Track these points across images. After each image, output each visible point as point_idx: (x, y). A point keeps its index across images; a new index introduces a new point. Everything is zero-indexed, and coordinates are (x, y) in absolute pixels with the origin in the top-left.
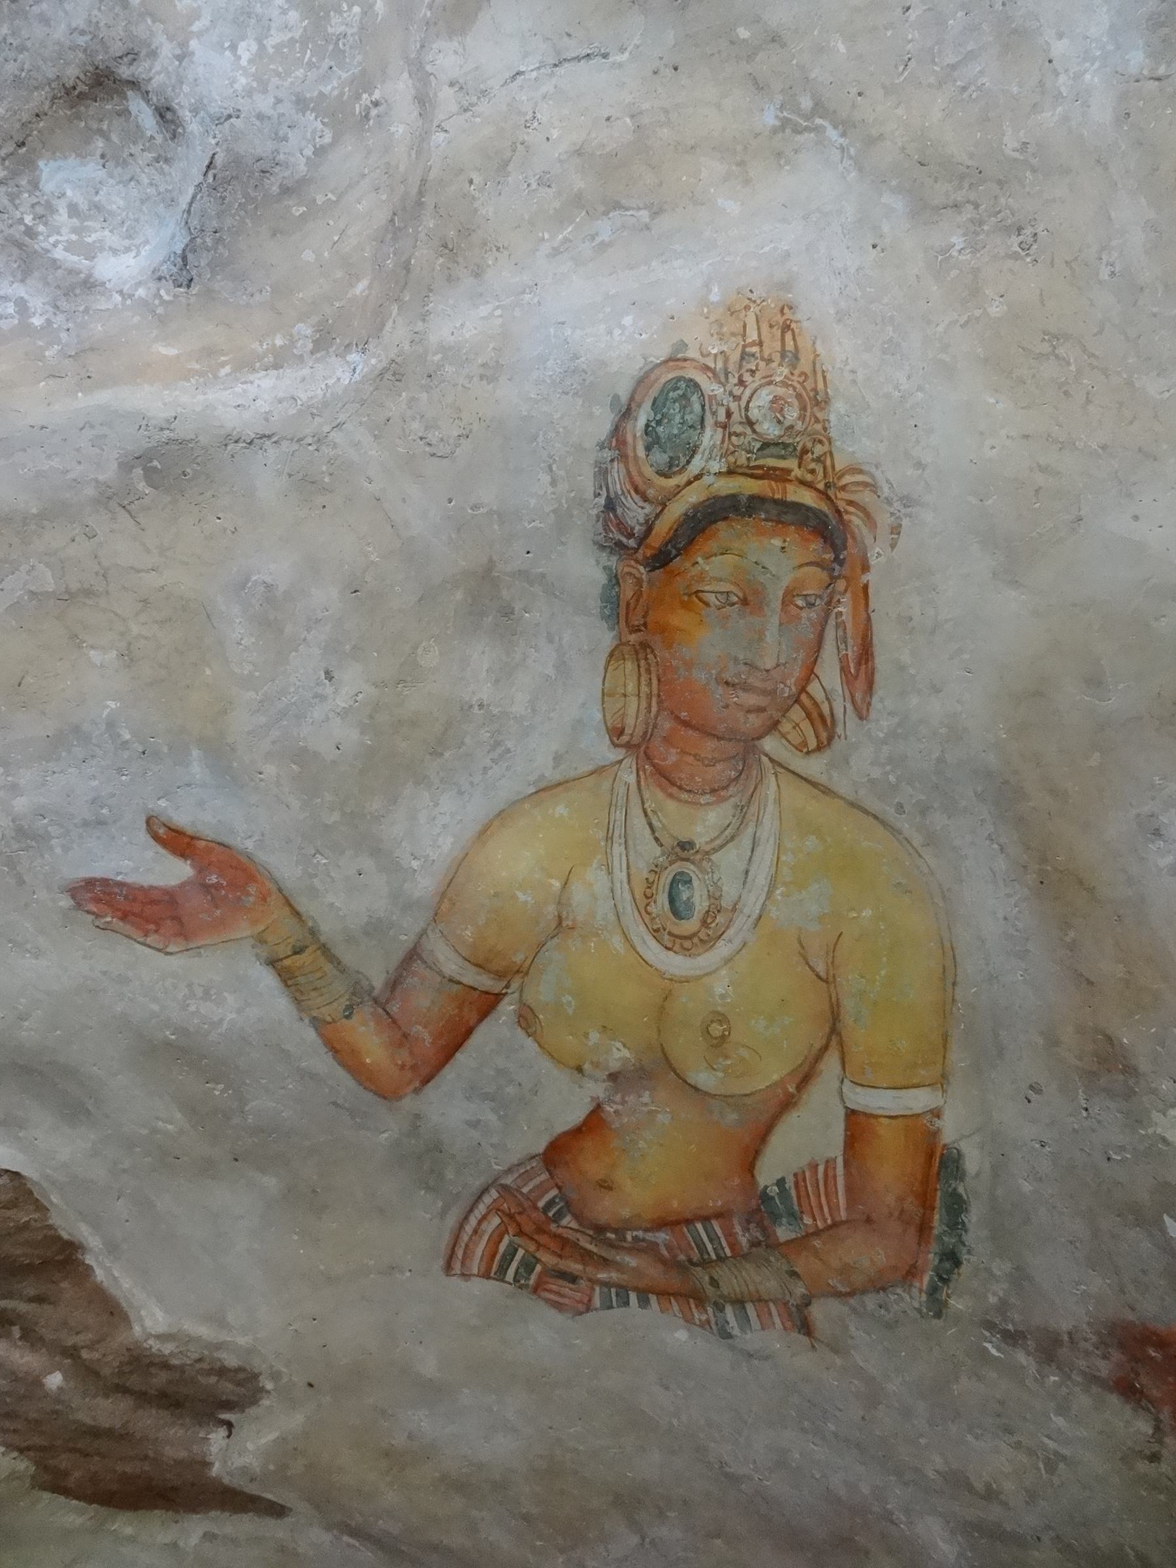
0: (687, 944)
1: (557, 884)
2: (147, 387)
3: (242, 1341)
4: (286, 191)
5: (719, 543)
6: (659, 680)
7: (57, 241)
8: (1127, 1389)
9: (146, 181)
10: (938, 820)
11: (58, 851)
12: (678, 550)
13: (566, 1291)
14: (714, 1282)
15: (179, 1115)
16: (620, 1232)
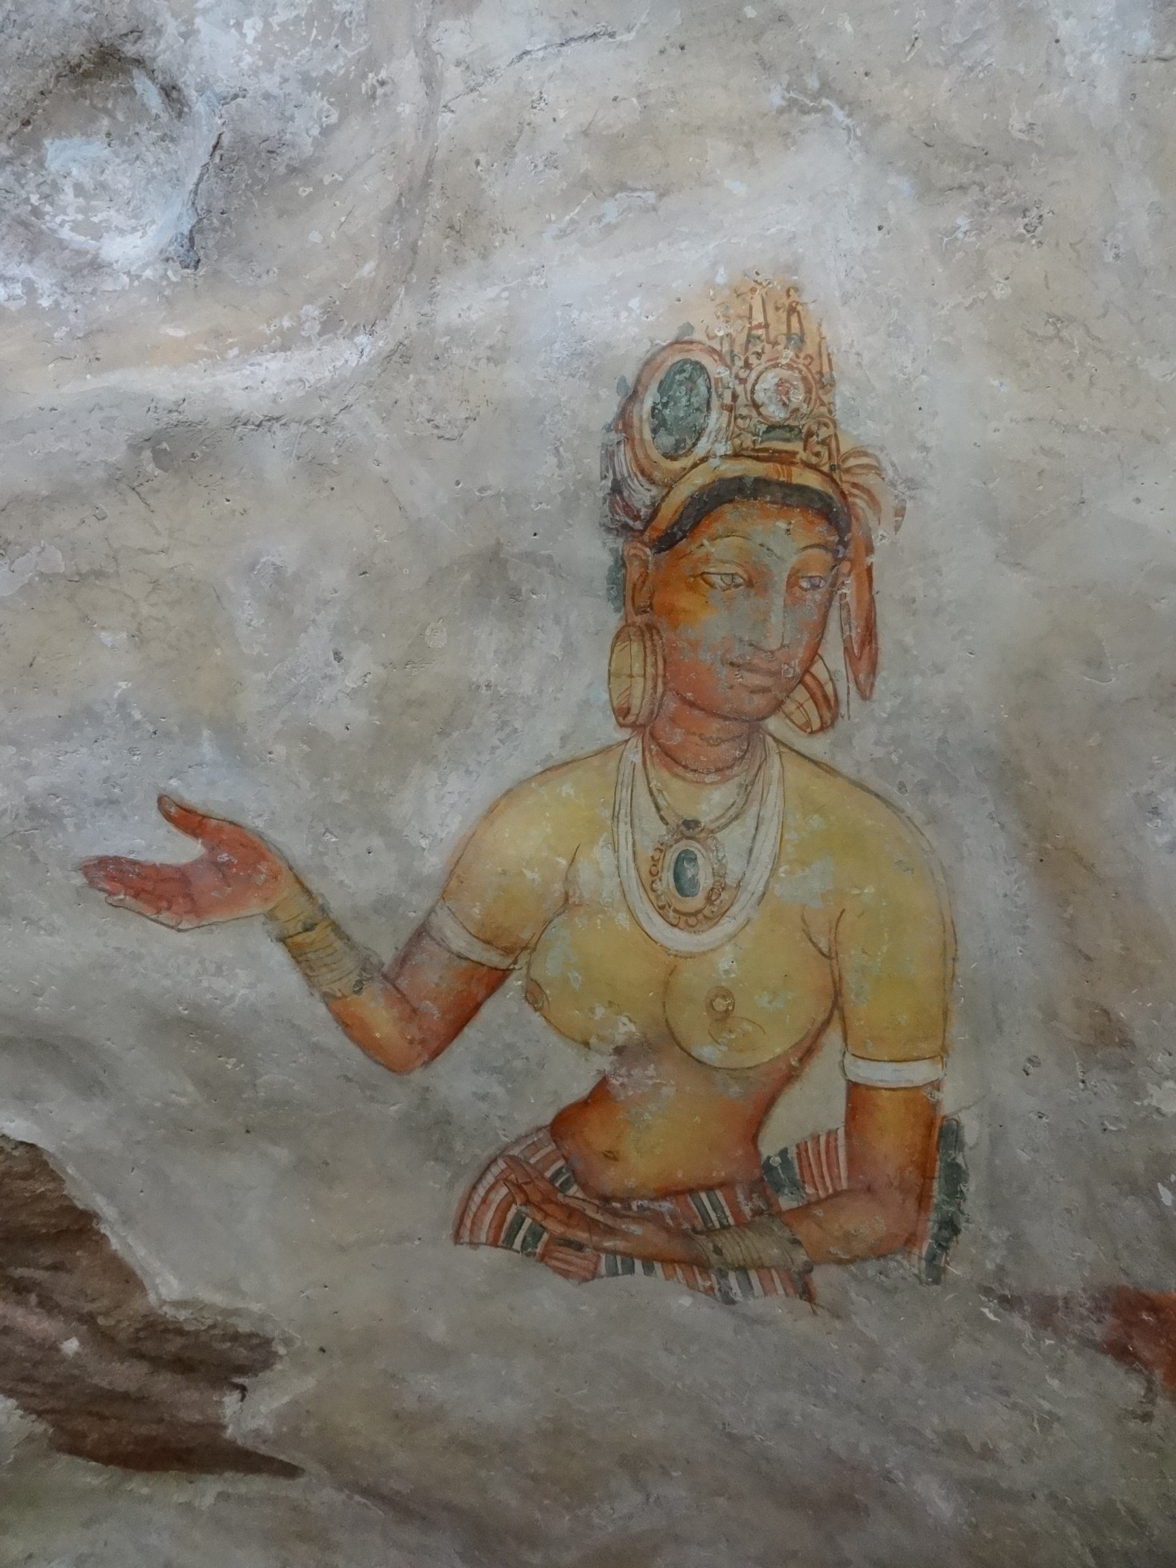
0: (692, 921)
1: (563, 862)
2: (156, 369)
3: (256, 1307)
4: (292, 170)
5: (724, 525)
6: (665, 661)
7: (63, 221)
8: (1121, 1352)
9: (151, 160)
11: (71, 829)
12: (684, 532)
13: (575, 1260)
14: (718, 1251)
15: (191, 1088)
16: (626, 1201)
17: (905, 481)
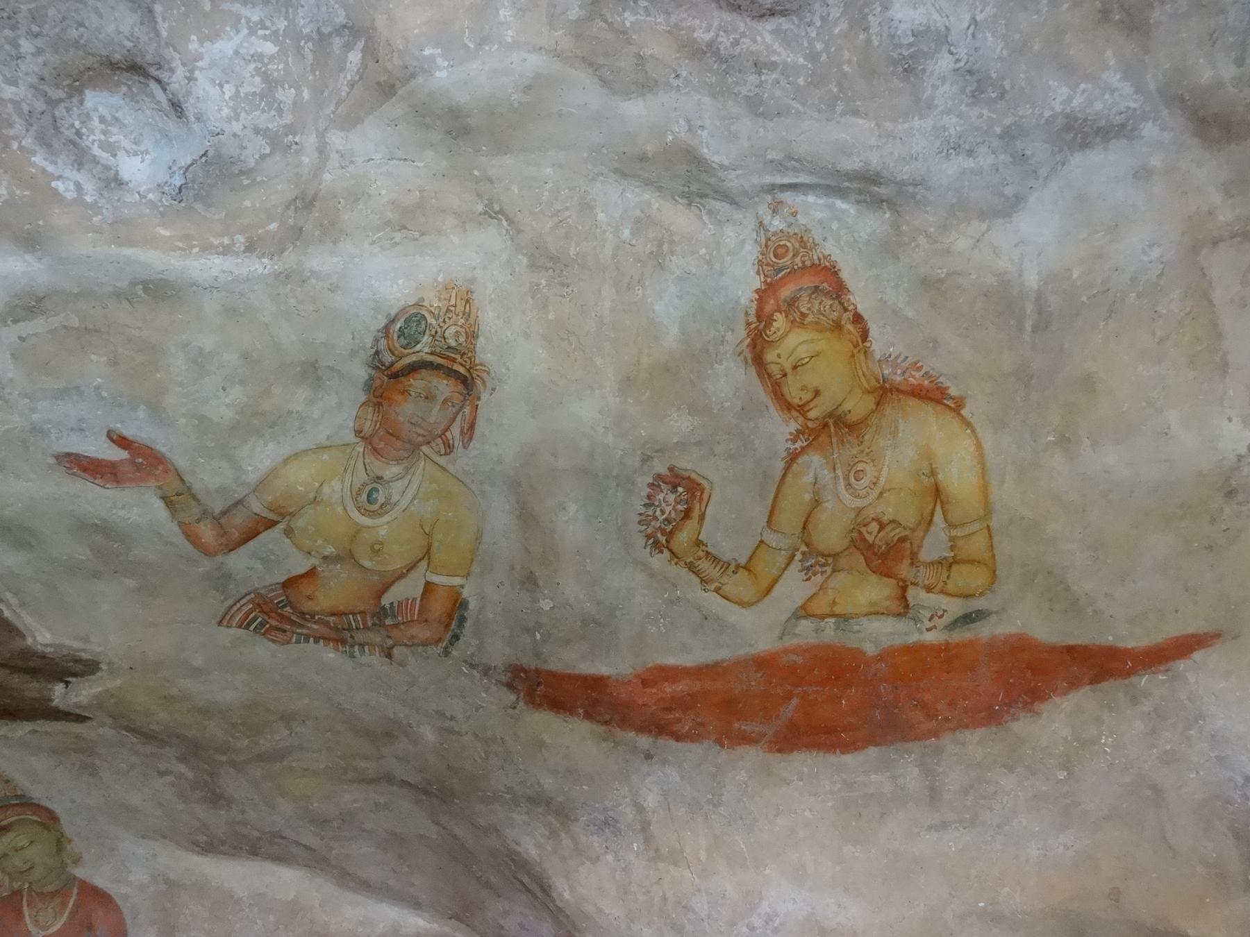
1: (317, 485)
4: (242, 172)
7: (93, 140)
8: (510, 686)
10: (487, 487)
14: (352, 637)
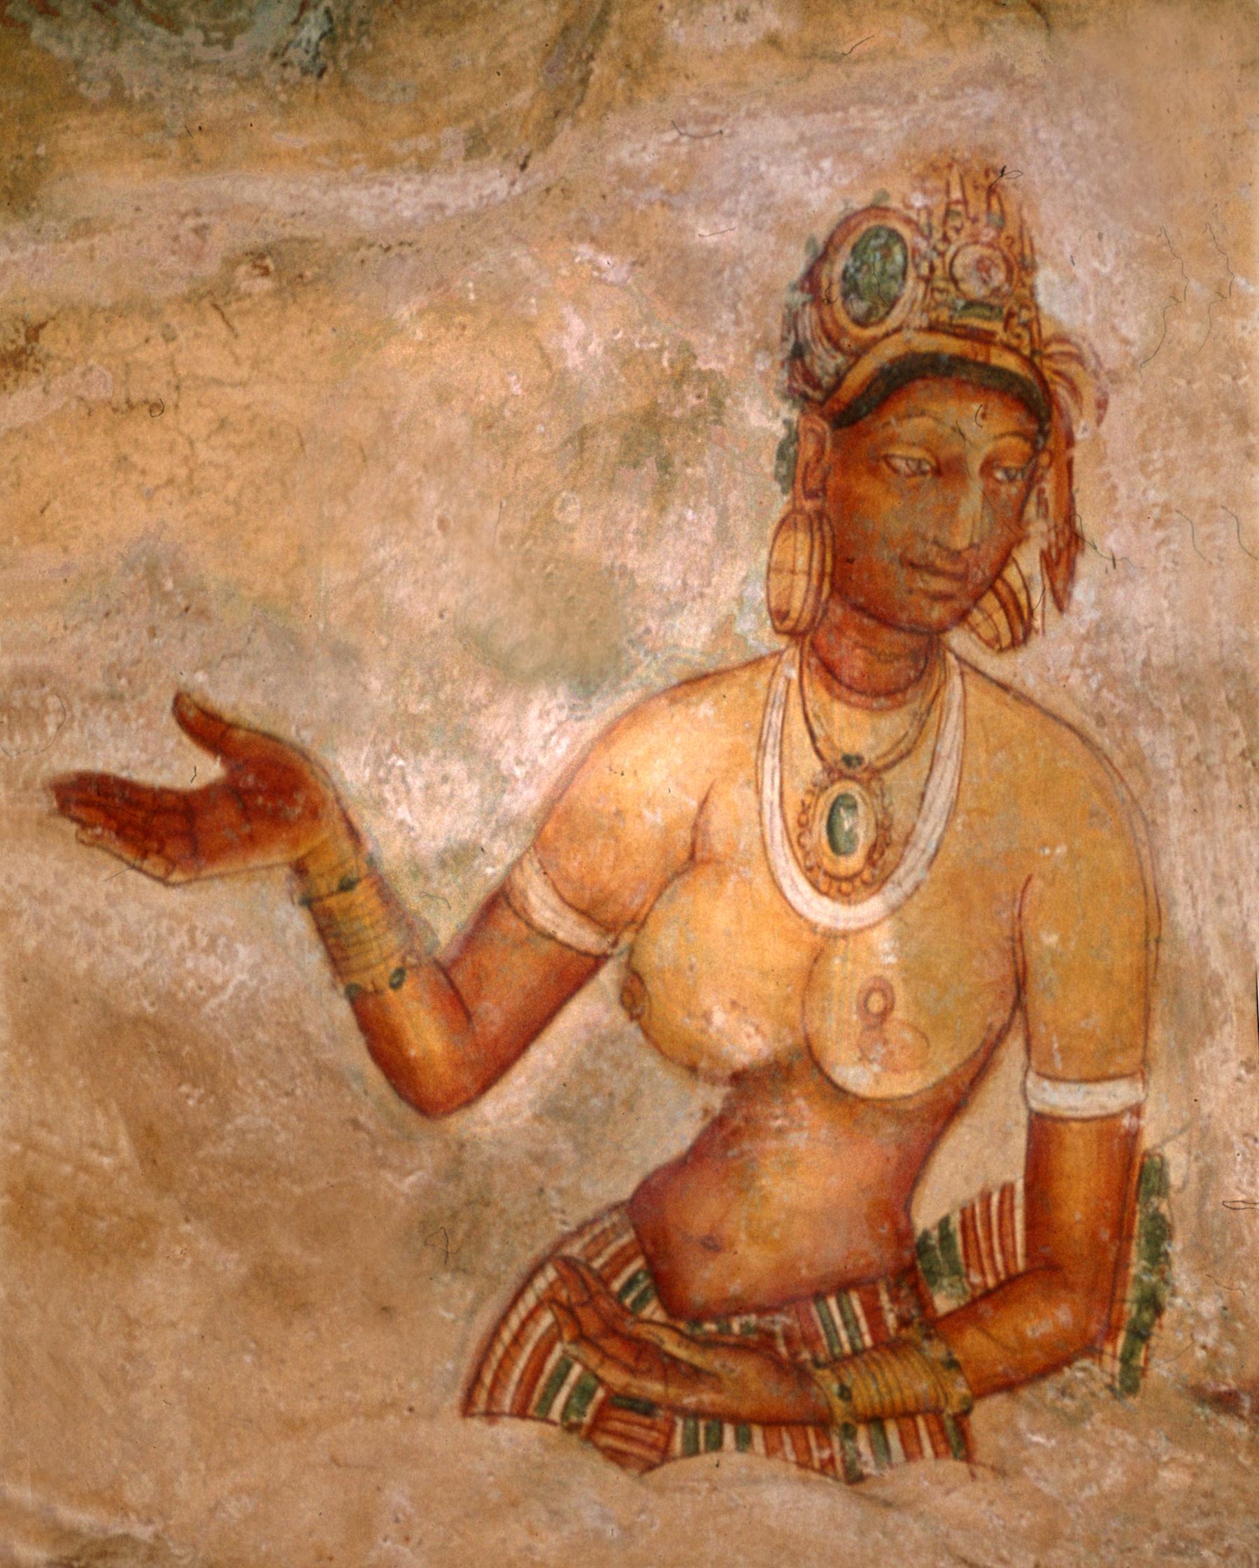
0: (845, 887)
1: (694, 804)
11: (51, 730)
13: (637, 1431)
14: (845, 1393)
17: (1108, 373)
